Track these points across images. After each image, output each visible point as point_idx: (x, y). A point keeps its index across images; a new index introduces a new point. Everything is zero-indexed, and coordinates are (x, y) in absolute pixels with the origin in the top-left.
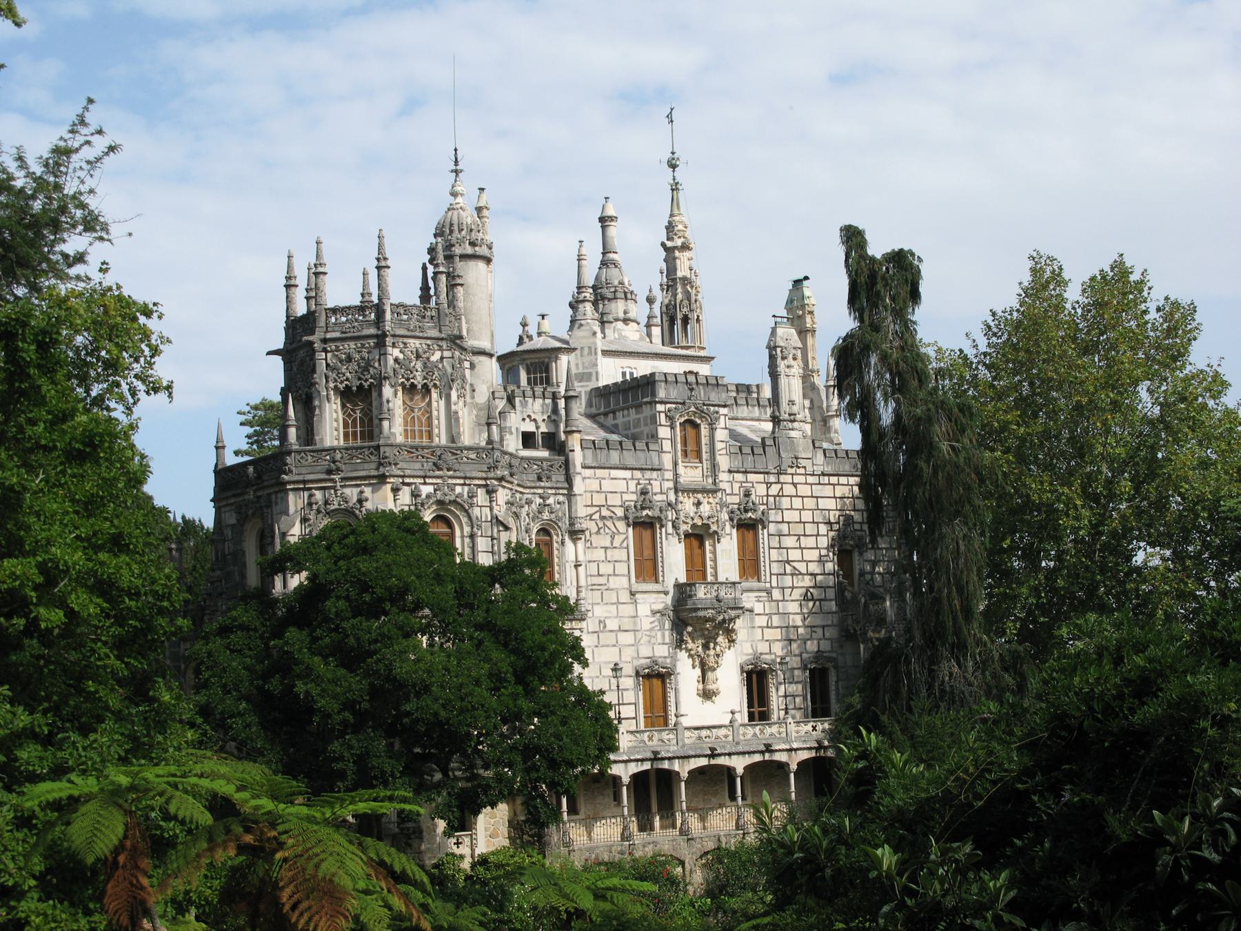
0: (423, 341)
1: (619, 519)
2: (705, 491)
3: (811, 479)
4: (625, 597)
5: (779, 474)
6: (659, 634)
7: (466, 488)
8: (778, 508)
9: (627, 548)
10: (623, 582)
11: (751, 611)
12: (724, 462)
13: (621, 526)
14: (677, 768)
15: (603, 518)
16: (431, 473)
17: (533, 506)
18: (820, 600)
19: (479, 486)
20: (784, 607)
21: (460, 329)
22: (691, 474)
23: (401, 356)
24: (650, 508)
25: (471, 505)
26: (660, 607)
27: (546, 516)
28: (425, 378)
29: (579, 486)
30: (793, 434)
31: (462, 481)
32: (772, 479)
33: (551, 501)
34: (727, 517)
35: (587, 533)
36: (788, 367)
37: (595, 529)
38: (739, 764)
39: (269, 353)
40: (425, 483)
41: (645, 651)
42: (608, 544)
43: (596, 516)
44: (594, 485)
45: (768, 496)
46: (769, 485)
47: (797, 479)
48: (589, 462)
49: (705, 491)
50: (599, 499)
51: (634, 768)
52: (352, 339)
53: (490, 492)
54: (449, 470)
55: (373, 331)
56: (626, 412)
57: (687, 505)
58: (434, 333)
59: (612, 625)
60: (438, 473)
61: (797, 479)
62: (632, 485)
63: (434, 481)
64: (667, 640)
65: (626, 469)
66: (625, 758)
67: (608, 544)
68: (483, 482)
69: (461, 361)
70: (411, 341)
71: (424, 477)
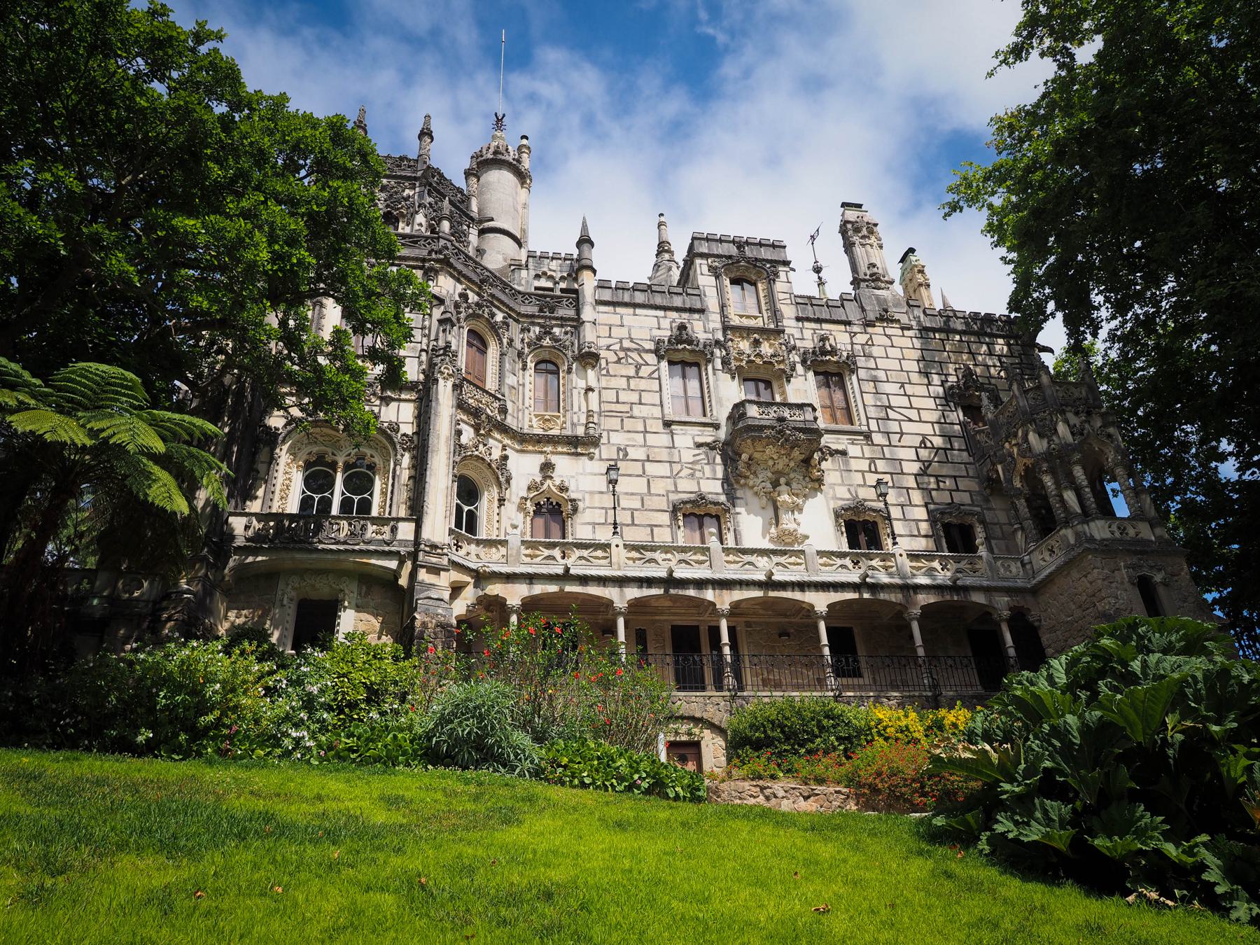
4: (659, 426)
6: (707, 468)
8: (868, 356)
9: (659, 379)
10: (657, 412)
11: (844, 453)
12: (788, 311)
13: (651, 358)
14: (709, 595)
15: (622, 349)
17: (532, 334)
18: (945, 449)
20: (891, 453)
28: (387, 206)
32: (856, 329)
33: (556, 331)
34: (797, 359)
35: (603, 362)
36: (863, 237)
38: (820, 602)
41: (687, 487)
43: (617, 347)
44: (615, 319)
45: (852, 344)
47: (889, 331)
49: (762, 331)
50: (617, 332)
51: (633, 593)
57: (745, 345)
59: (632, 453)
61: (889, 331)
62: (665, 324)
64: (720, 474)
66: (619, 573)
67: (632, 372)
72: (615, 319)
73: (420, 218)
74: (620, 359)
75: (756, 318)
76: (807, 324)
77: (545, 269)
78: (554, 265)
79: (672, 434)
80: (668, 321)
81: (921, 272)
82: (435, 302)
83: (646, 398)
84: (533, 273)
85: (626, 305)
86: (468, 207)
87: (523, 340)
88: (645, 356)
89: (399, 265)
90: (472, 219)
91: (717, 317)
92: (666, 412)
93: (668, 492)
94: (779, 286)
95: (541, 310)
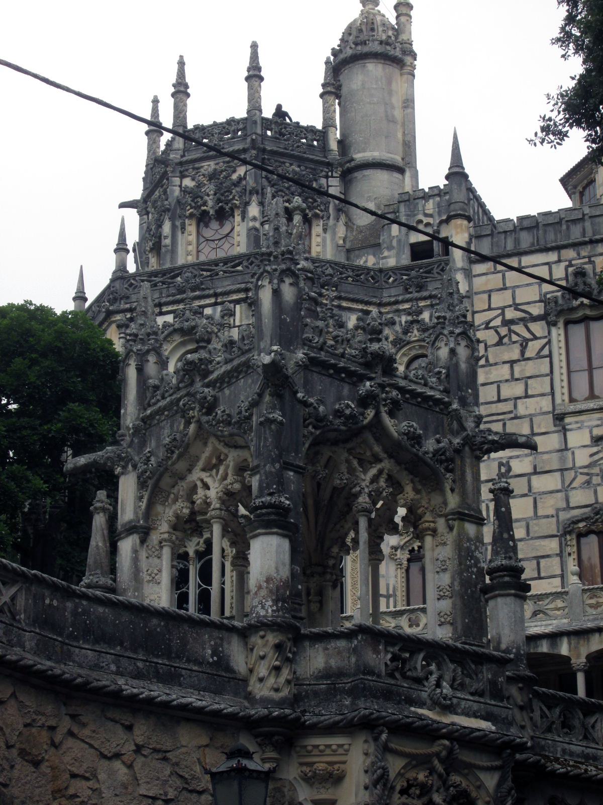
1: (535, 319)
7: (219, 308)
9: (550, 356)
10: (545, 404)
13: (538, 328)
14: (564, 649)
15: (507, 323)
17: (397, 328)
19: (237, 302)
31: (213, 300)
33: (426, 316)
40: (161, 314)
41: (580, 497)
42: (515, 354)
43: (497, 322)
50: (499, 300)
62: (559, 272)
63: (175, 307)
65: (547, 250)
67: (515, 354)
68: (242, 295)
70: (205, 164)
72: (495, 281)
73: (254, 210)
74: (501, 338)
77: (421, 217)
78: (430, 206)
79: (564, 430)
80: (563, 265)
83: (536, 386)
86: (324, 147)
88: (532, 326)
89: (222, 303)
90: (329, 165)
92: (558, 400)
93: (558, 510)
95: (406, 290)
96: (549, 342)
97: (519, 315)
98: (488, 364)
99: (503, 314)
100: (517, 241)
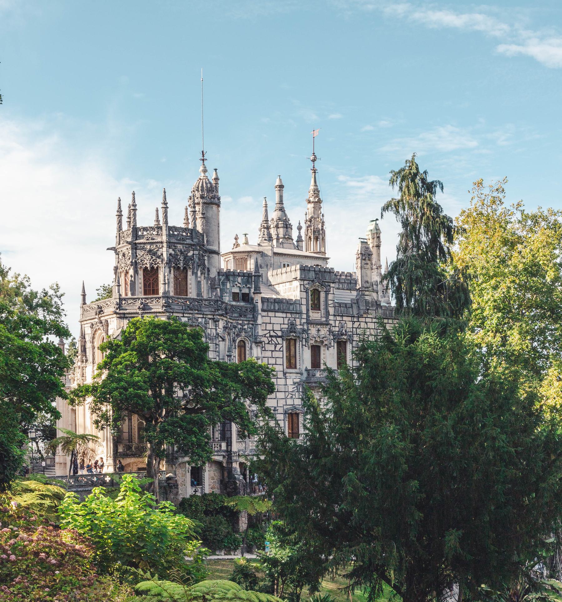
0: (185, 246)
2: (321, 324)
3: (374, 320)
5: (358, 317)
7: (204, 320)
9: (283, 351)
12: (332, 311)
13: (280, 340)
15: (271, 336)
16: (187, 312)
17: (237, 329)
19: (210, 319)
21: (203, 239)
22: (315, 316)
23: (173, 253)
24: (295, 332)
25: (206, 328)
26: (298, 380)
27: (243, 334)
29: (260, 321)
30: (367, 298)
31: (202, 316)
33: (246, 327)
34: (332, 338)
35: (263, 343)
37: (267, 342)
39: (108, 249)
40: (183, 317)
41: (290, 402)
42: (273, 349)
43: (268, 335)
44: (267, 320)
45: (353, 328)
46: (354, 322)
47: (368, 320)
48: (265, 308)
50: (269, 327)
52: (149, 243)
53: (216, 321)
54: (195, 310)
55: (159, 240)
56: (284, 284)
57: (313, 331)
58: (189, 241)
60: (190, 312)
61: (368, 320)
63: (188, 315)
65: (283, 312)
69: (203, 256)
71: (183, 313)
72: (267, 320)
75: (318, 313)
76: (337, 317)
77: (236, 283)
79: (286, 378)
81: (379, 237)
82: (220, 339)
84: (232, 285)
85: (272, 312)
87: (234, 333)
91: (304, 316)
94: (330, 297)
96: (282, 346)
97: (275, 334)
98: (265, 350)
99: (270, 333)
100: (274, 306)
